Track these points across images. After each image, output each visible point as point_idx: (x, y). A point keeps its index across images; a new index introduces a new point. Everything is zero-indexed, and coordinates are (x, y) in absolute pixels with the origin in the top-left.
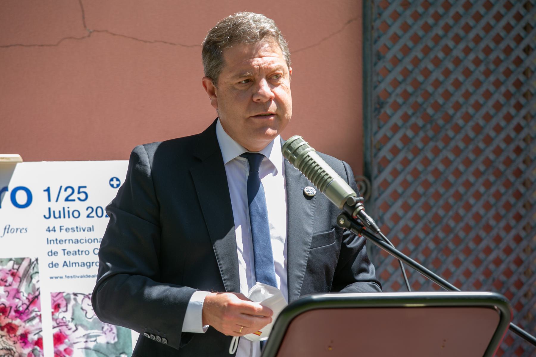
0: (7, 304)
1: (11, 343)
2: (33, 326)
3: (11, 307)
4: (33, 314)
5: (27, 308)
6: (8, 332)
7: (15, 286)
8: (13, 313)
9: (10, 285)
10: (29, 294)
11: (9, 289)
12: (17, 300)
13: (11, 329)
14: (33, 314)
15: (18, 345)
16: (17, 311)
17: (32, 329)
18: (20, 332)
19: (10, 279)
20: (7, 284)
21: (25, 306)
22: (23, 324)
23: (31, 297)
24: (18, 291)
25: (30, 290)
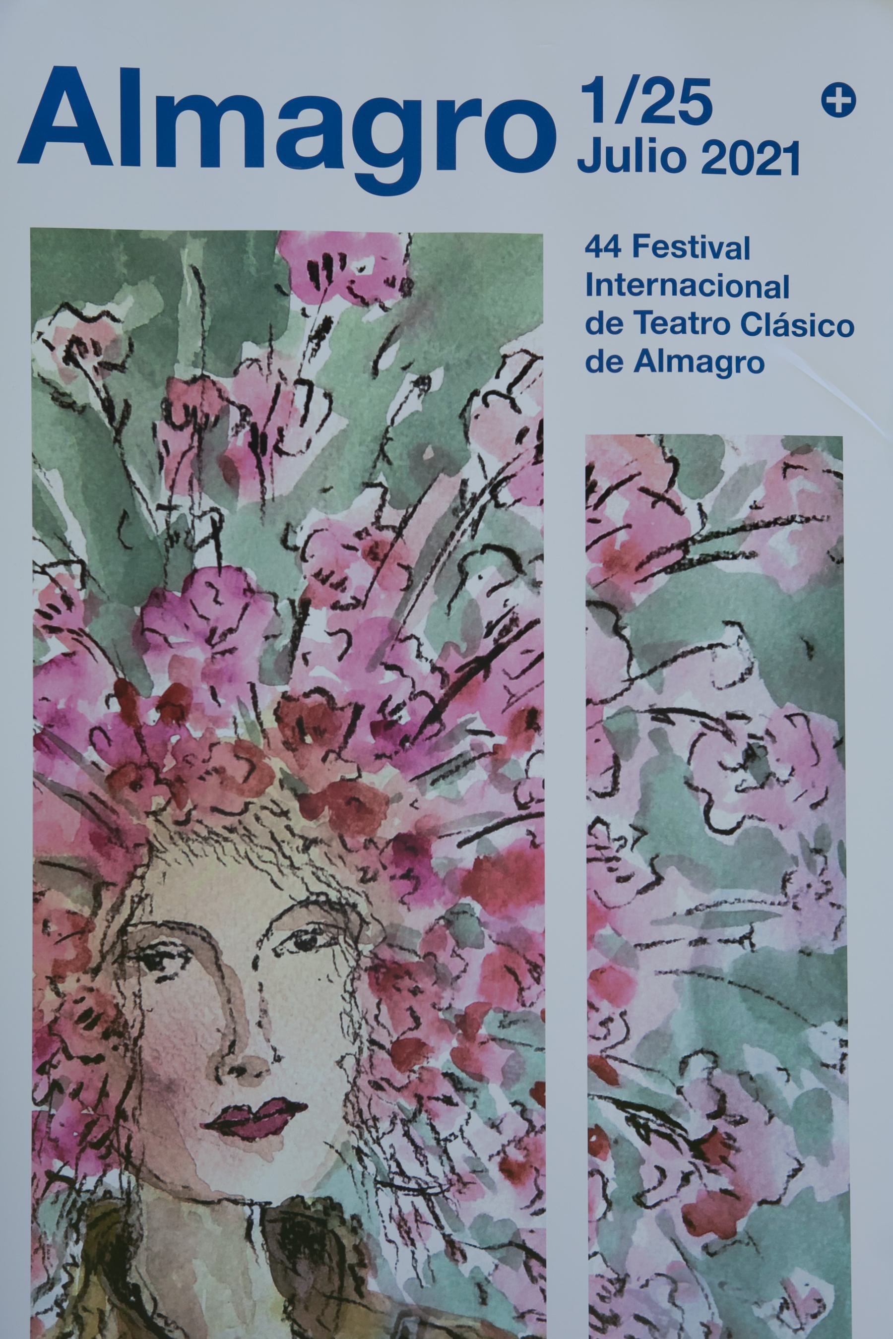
0: (342, 691)
1: (351, 878)
2: (458, 801)
3: (358, 709)
4: (464, 745)
5: (435, 716)
6: (337, 823)
7: (383, 606)
8: (364, 736)
9: (358, 603)
10: (446, 647)
11: (351, 620)
12: (390, 676)
13: (351, 807)
14: (464, 745)
15: (381, 888)
16: (383, 727)
17: (452, 814)
18: (393, 825)
19: (359, 573)
20: (345, 599)
21: (424, 707)
22: (412, 791)
23: (453, 663)
24: (396, 635)
25: (453, 631)
